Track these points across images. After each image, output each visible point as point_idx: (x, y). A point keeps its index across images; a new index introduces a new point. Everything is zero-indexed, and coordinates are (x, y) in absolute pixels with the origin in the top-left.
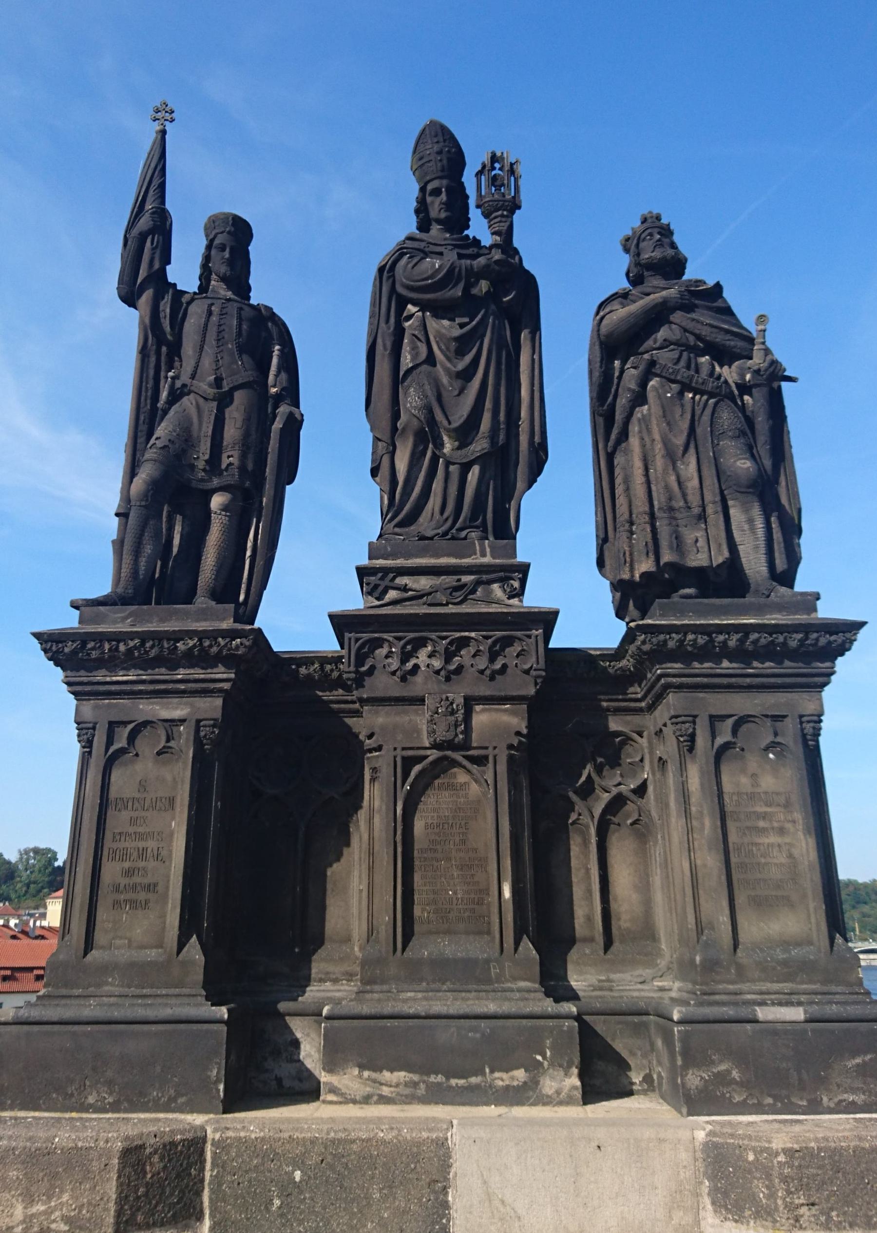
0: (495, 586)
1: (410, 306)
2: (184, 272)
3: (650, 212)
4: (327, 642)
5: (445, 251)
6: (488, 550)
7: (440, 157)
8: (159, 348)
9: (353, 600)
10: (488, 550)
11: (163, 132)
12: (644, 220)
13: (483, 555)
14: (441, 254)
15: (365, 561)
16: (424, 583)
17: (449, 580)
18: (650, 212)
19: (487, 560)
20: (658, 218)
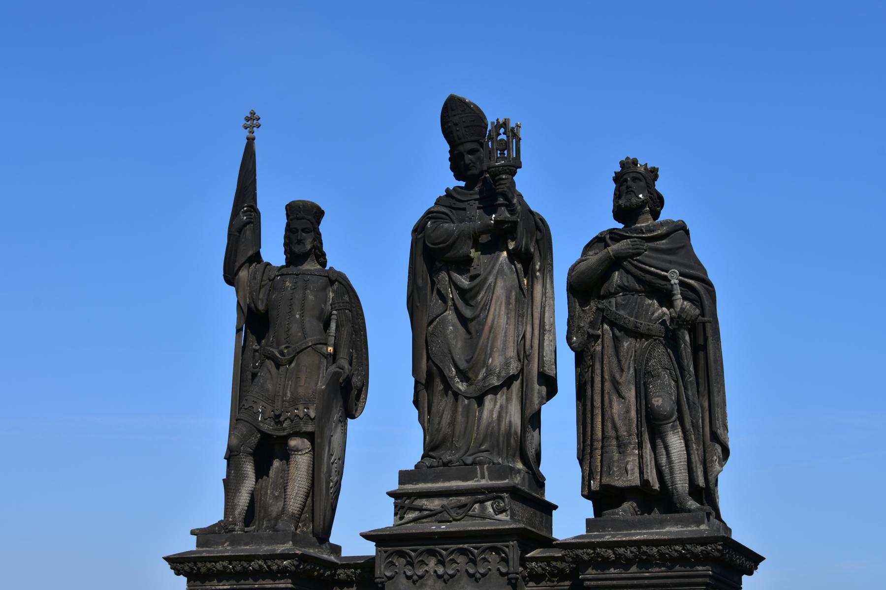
0: (489, 503)
1: (437, 263)
2: (273, 252)
3: (628, 158)
4: (369, 549)
5: (467, 207)
6: (486, 474)
7: (462, 125)
8: (255, 322)
9: (385, 518)
10: (486, 474)
11: (250, 141)
12: (622, 164)
13: (483, 477)
14: (464, 209)
15: (395, 486)
16: (435, 504)
17: (454, 500)
18: (628, 158)
19: (484, 482)
20: (635, 162)
